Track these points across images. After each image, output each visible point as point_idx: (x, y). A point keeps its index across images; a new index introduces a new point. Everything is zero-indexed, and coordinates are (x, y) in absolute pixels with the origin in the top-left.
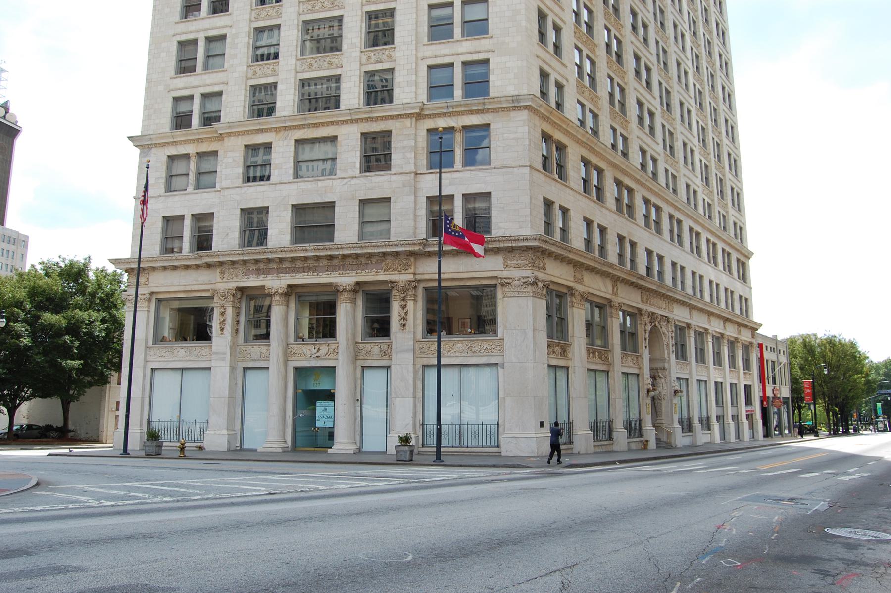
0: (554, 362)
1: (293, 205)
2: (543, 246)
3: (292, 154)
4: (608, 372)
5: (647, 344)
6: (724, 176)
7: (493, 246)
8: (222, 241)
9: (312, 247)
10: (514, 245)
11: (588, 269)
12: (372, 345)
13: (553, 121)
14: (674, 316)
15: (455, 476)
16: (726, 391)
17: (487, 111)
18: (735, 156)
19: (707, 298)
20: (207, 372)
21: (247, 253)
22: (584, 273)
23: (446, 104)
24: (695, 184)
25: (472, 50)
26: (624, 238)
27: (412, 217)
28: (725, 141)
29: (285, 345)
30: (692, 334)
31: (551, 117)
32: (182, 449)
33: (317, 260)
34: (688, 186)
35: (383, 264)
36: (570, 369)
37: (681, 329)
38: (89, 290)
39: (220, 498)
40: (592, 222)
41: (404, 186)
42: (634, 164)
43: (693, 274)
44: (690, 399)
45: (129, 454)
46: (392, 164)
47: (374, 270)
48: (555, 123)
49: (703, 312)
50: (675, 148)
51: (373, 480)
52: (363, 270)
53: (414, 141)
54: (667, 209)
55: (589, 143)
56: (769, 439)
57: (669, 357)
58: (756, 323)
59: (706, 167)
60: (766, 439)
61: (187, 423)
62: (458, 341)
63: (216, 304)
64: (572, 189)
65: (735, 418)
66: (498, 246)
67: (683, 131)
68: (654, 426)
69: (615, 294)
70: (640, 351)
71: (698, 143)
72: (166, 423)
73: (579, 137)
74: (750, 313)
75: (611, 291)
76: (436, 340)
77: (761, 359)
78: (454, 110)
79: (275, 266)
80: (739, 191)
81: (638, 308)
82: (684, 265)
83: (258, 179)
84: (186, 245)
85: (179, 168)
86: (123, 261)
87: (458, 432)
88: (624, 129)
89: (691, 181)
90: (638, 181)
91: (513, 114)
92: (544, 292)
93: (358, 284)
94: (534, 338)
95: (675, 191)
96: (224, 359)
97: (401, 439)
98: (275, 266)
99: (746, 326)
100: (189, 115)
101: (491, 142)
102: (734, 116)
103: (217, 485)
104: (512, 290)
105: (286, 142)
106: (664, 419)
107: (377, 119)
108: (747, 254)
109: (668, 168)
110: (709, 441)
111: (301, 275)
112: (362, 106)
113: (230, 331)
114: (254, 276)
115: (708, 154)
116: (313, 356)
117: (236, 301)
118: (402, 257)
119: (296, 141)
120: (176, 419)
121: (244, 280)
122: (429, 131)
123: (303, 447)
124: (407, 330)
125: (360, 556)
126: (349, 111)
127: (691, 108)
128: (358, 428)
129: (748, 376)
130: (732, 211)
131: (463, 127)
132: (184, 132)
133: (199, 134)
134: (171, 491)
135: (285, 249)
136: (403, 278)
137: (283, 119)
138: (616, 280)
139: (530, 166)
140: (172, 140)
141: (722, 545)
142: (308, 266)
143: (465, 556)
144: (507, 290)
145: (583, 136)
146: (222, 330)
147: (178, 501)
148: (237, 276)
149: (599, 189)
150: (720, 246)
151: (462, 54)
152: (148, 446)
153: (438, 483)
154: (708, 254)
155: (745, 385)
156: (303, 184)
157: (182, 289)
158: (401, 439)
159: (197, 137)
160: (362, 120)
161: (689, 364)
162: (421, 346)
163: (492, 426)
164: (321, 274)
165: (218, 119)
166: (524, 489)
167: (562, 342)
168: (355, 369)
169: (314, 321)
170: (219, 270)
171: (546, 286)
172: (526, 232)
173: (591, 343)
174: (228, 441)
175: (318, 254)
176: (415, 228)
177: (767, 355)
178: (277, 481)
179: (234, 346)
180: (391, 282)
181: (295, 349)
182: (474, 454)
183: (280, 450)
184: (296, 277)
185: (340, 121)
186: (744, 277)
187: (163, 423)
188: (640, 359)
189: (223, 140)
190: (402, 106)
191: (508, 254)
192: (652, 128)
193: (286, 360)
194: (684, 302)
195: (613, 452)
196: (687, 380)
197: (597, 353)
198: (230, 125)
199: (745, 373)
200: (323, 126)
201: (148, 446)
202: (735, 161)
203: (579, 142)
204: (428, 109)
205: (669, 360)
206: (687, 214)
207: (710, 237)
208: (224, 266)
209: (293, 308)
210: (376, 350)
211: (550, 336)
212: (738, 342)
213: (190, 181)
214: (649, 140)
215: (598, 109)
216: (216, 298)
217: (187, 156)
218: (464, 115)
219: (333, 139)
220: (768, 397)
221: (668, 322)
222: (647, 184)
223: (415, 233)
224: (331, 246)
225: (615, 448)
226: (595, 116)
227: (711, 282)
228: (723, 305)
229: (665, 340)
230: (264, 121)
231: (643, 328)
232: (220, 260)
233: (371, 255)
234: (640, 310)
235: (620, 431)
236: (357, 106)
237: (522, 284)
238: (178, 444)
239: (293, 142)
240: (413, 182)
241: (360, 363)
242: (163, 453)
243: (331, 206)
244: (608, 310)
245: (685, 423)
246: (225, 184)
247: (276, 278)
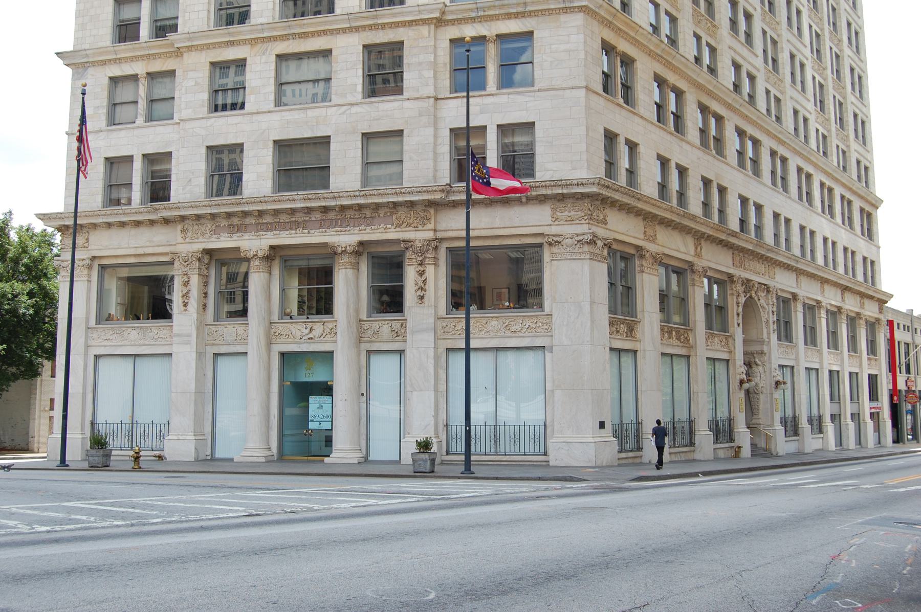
0: (618, 344)
1: (275, 141)
2: (604, 192)
3: (273, 74)
4: (688, 357)
5: (740, 321)
6: (844, 98)
7: (538, 193)
8: (183, 189)
9: (301, 196)
10: (565, 191)
11: (663, 223)
12: (380, 323)
13: (616, 26)
14: (776, 284)
15: (490, 492)
16: (844, 383)
17: (530, 14)
18: (860, 72)
19: (820, 260)
20: (166, 359)
21: (215, 205)
22: (658, 228)
23: (474, 6)
24: (806, 109)
26: (710, 181)
27: (431, 155)
28: (847, 52)
29: (267, 324)
30: (800, 308)
31: (614, 21)
32: (137, 458)
33: (309, 213)
34: (796, 112)
35: (394, 217)
36: (638, 353)
37: (786, 301)
38: (10, 255)
39: (187, 521)
40: (668, 160)
41: (420, 115)
42: (725, 83)
43: (802, 228)
44: (796, 393)
45: (68, 466)
46: (404, 86)
47: (382, 225)
48: (620, 29)
49: (815, 279)
50: (780, 61)
51: (384, 497)
52: (368, 225)
53: (433, 55)
54: (767, 143)
55: (665, 56)
56: (901, 445)
57: (769, 338)
58: (885, 293)
59: (821, 86)
60: (896, 445)
61: (143, 425)
62: (492, 317)
63: (177, 271)
64: (642, 117)
65: (856, 417)
66: (544, 193)
67: (790, 39)
68: (748, 428)
69: (698, 255)
70: (731, 329)
71: (810, 54)
72: (116, 425)
73: (652, 48)
74: (877, 280)
75: (692, 252)
76: (464, 316)
77: (891, 341)
78: (486, 13)
79: (253, 222)
80: (865, 118)
81: (728, 274)
82: (789, 217)
83: (229, 107)
84: (137, 194)
85: (125, 93)
86: (54, 216)
87: (493, 437)
88: (711, 36)
89: (801, 105)
90: (729, 106)
91: (563, 18)
92: (605, 253)
93: (361, 243)
94: (592, 312)
95: (778, 119)
96: (188, 343)
97: (419, 444)
98: (253, 222)
99: (871, 298)
100: (136, 23)
101: (535, 56)
102: (859, 18)
103: (182, 505)
104: (563, 251)
105: (264, 59)
106: (762, 418)
107: (384, 26)
108: (874, 202)
109: (770, 88)
110: (821, 448)
111: (287, 232)
112: (363, 9)
113: (196, 306)
114: (226, 235)
115: (824, 69)
116: (304, 338)
117: (203, 267)
118: (419, 208)
119: (278, 56)
120: (127, 420)
121: (213, 239)
122: (452, 41)
123: (292, 455)
124: (426, 304)
125: (369, 593)
126: (346, 16)
127: (801, 8)
128: (363, 431)
129: (873, 362)
130: (854, 146)
131: (497, 36)
132: (130, 46)
133: (150, 48)
134: (123, 512)
135: (266, 199)
136: (420, 235)
137: (260, 27)
138: (699, 237)
139: (587, 88)
140: (114, 57)
141: (838, 581)
142: (295, 222)
143: (504, 593)
144: (557, 251)
145: (657, 46)
146: (185, 305)
147: (132, 525)
148: (203, 234)
149: (678, 117)
150: (838, 191)
152: (92, 456)
153: (466, 501)
154: (822, 202)
155: (869, 375)
156: (288, 113)
157: (133, 252)
158: (419, 444)
159: (147, 52)
160: (364, 28)
161: (796, 346)
162: (444, 324)
163: (537, 427)
164: (313, 231)
165: (174, 28)
166: (579, 508)
167: (628, 318)
168: (359, 355)
169: (305, 293)
170: (179, 227)
171: (608, 246)
172: (582, 174)
173: (667, 320)
174: (195, 448)
175: (309, 205)
176: (436, 170)
177: (899, 335)
178: (260, 498)
179: (201, 325)
180: (404, 241)
181: (281, 328)
182: (514, 463)
183: (263, 460)
184: (281, 236)
185: (336, 30)
186: (869, 233)
187: (112, 425)
188: (730, 340)
189: (182, 55)
190: (417, 8)
191: (558, 204)
192: (748, 35)
193: (269, 344)
194: (789, 265)
195: (694, 460)
196: (792, 367)
197: (674, 333)
198: (190, 35)
199: (869, 359)
200: (313, 36)
201: (92, 456)
202: (860, 78)
203: (651, 54)
204: (452, 12)
205: (769, 342)
206: (795, 149)
207: (824, 180)
208: (187, 222)
209: (277, 276)
210: (386, 329)
211: (613, 311)
212: (860, 318)
213: (139, 110)
214: (745, 52)
215: (677, 10)
216: (177, 264)
217: (134, 78)
218: (498, 19)
219: (326, 54)
220: (900, 390)
221: (768, 291)
222: (742, 109)
223: (435, 177)
224: (325, 195)
225: (698, 456)
226: (673, 20)
227: (825, 240)
228: (841, 270)
229: (764, 317)
230: (235, 30)
231: (735, 300)
232: (181, 214)
233: (377, 207)
234: (730, 276)
235: (704, 434)
236: (357, 10)
237: (576, 242)
238: (132, 453)
239: (273, 58)
240: (432, 109)
241: (365, 347)
242: (111, 464)
243: (325, 141)
244: (689, 277)
245: (789, 424)
246: (185, 114)
247: (255, 237)
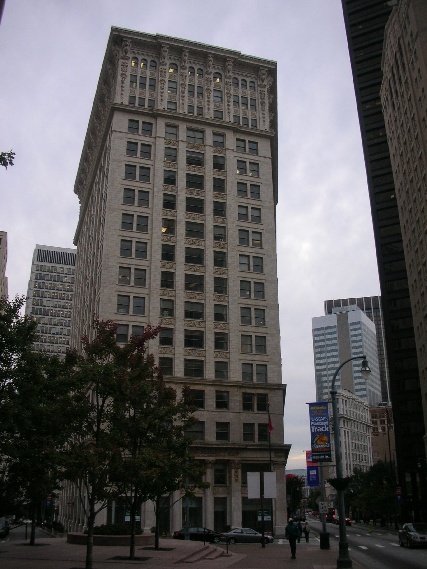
91: (277, 391)
93: (217, 460)
107: (223, 386)
131: (257, 394)
210: (221, 489)
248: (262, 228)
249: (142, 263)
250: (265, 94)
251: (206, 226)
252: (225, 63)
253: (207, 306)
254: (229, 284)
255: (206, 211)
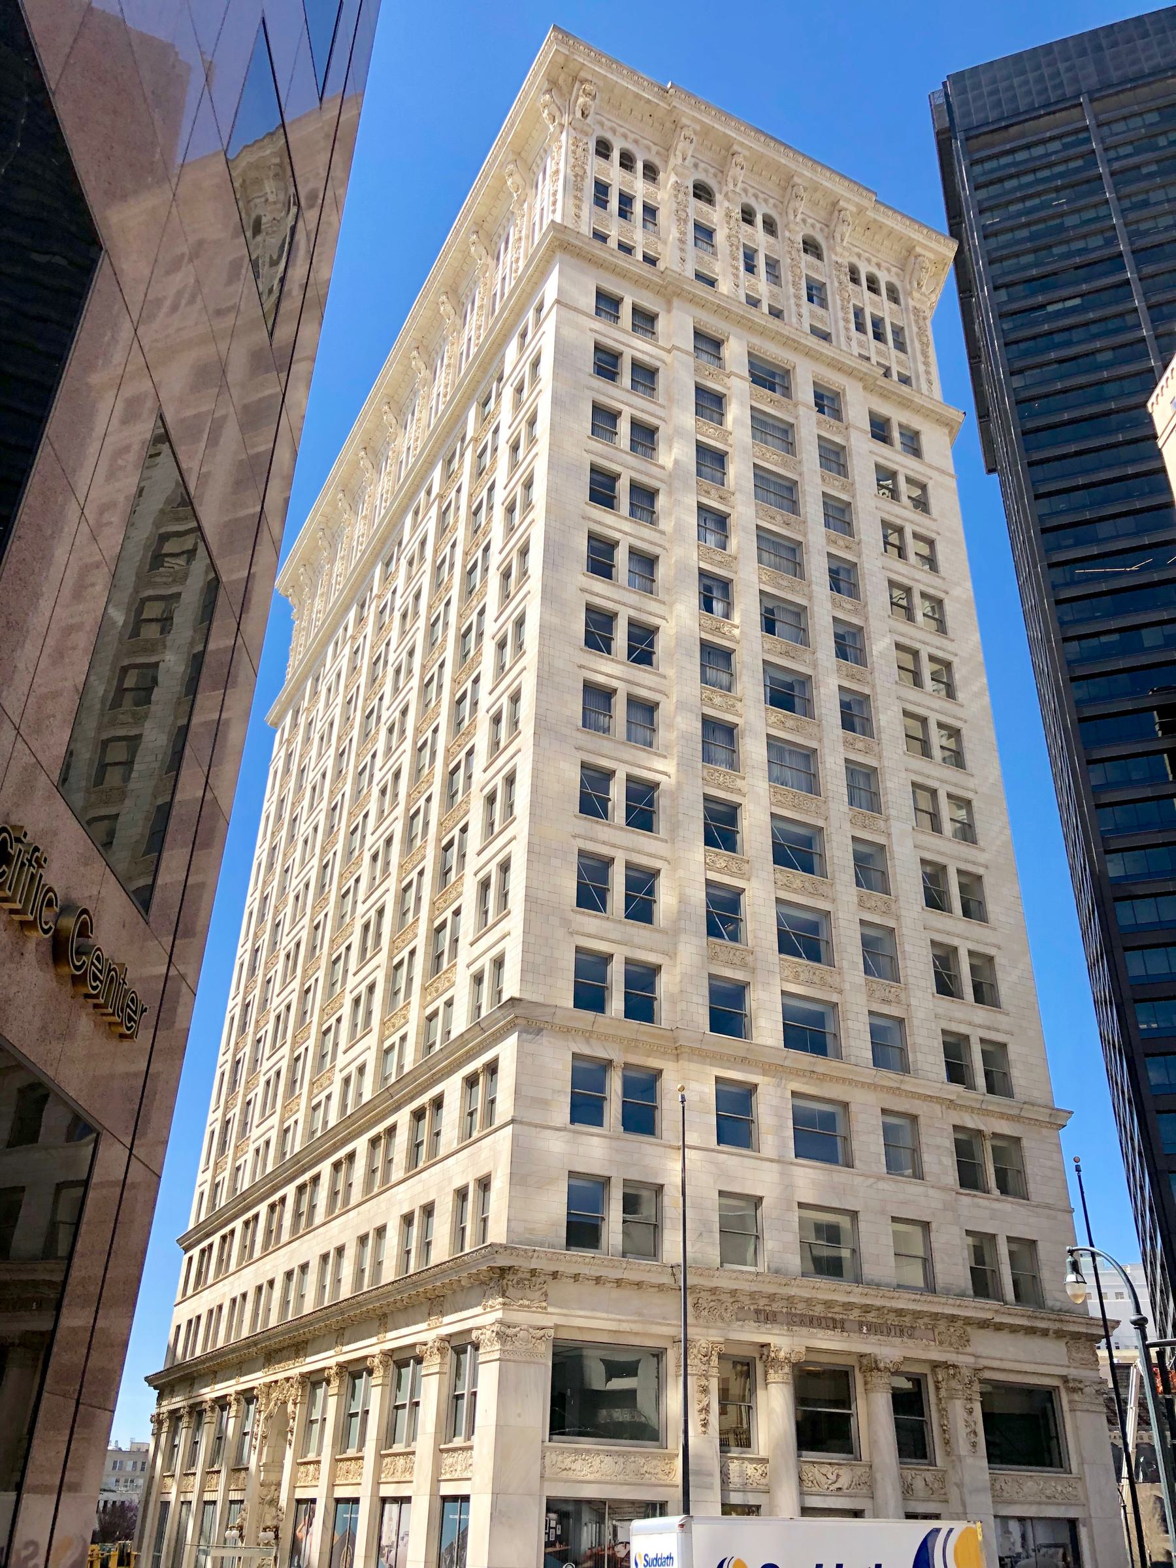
25: (988, 1023)
41: (945, 1209)
118: (960, 1323)
151: (980, 1026)
156: (811, 1170)
164: (852, 1334)
180: (955, 1366)
200: (831, 1080)
248: (950, 649)
249: (643, 682)
250: (925, 318)
251: (816, 615)
252: (832, 213)
253: (834, 837)
254: (889, 784)
255: (813, 572)
